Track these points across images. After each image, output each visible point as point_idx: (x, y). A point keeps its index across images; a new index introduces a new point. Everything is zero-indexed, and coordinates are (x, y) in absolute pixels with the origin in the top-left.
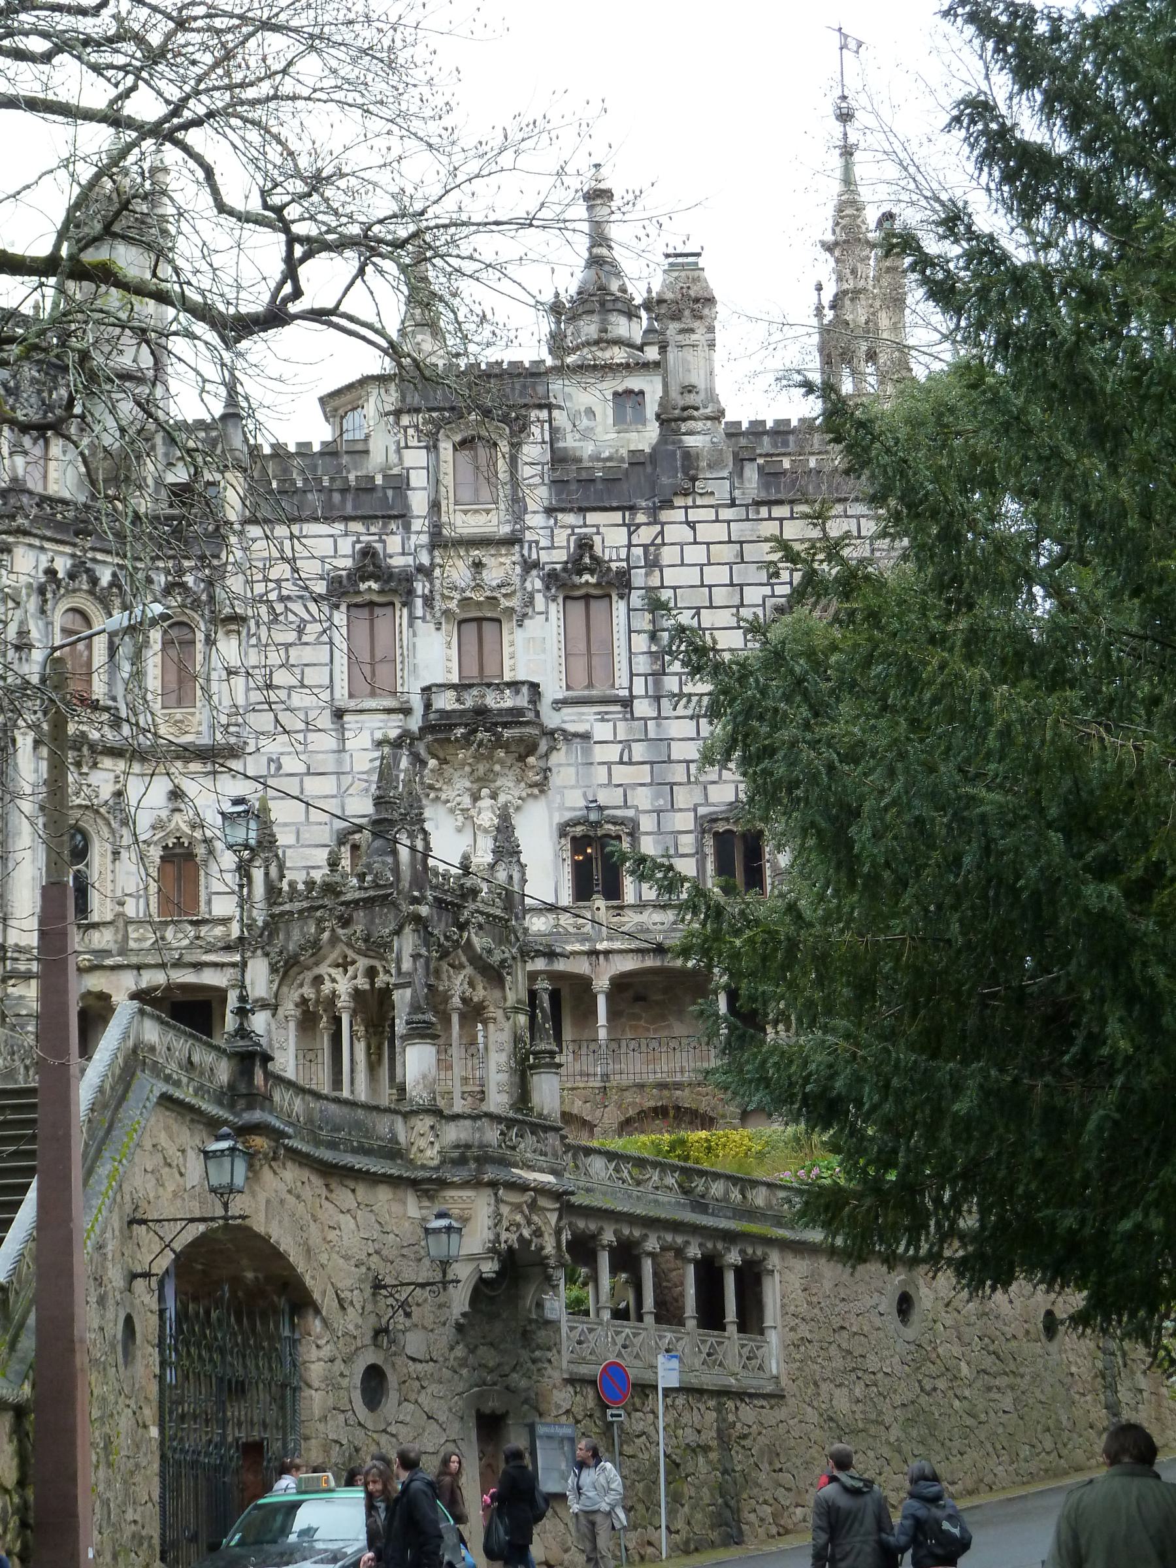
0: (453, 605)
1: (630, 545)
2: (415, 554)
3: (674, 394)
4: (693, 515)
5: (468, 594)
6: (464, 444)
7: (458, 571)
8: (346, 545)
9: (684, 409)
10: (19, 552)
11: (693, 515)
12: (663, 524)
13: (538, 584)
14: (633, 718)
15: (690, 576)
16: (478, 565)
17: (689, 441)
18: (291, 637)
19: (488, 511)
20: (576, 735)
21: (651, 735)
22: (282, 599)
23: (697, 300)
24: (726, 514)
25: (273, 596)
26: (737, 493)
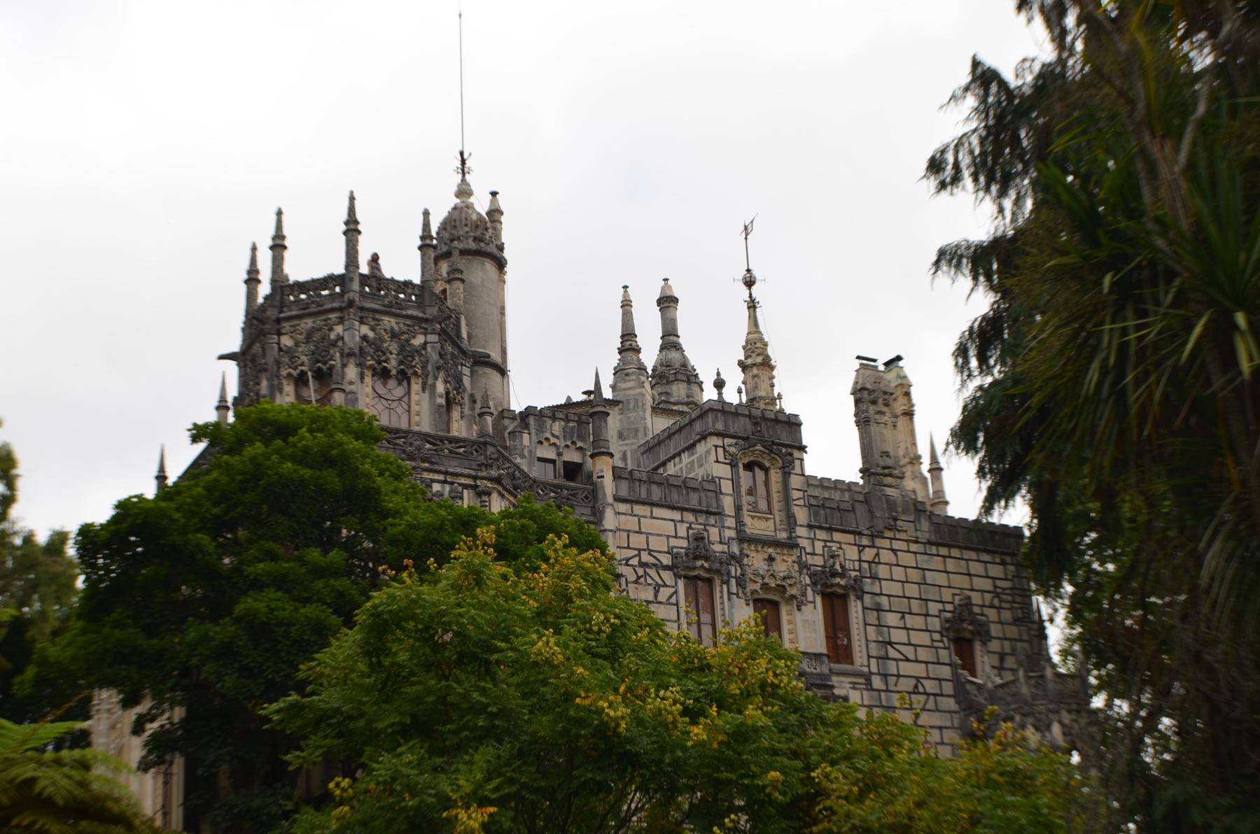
0: (757, 587)
1: (860, 561)
2: (728, 544)
3: (876, 456)
4: (897, 545)
5: (766, 580)
6: (749, 467)
7: (756, 560)
8: (682, 529)
9: (884, 468)
10: (495, 495)
11: (897, 545)
12: (878, 548)
13: (808, 581)
14: (873, 690)
15: (895, 589)
16: (771, 559)
17: (889, 491)
18: (651, 597)
19: (767, 519)
20: (839, 697)
21: (884, 703)
22: (643, 565)
23: (885, 393)
24: (914, 547)
25: (635, 561)
26: (919, 534)
